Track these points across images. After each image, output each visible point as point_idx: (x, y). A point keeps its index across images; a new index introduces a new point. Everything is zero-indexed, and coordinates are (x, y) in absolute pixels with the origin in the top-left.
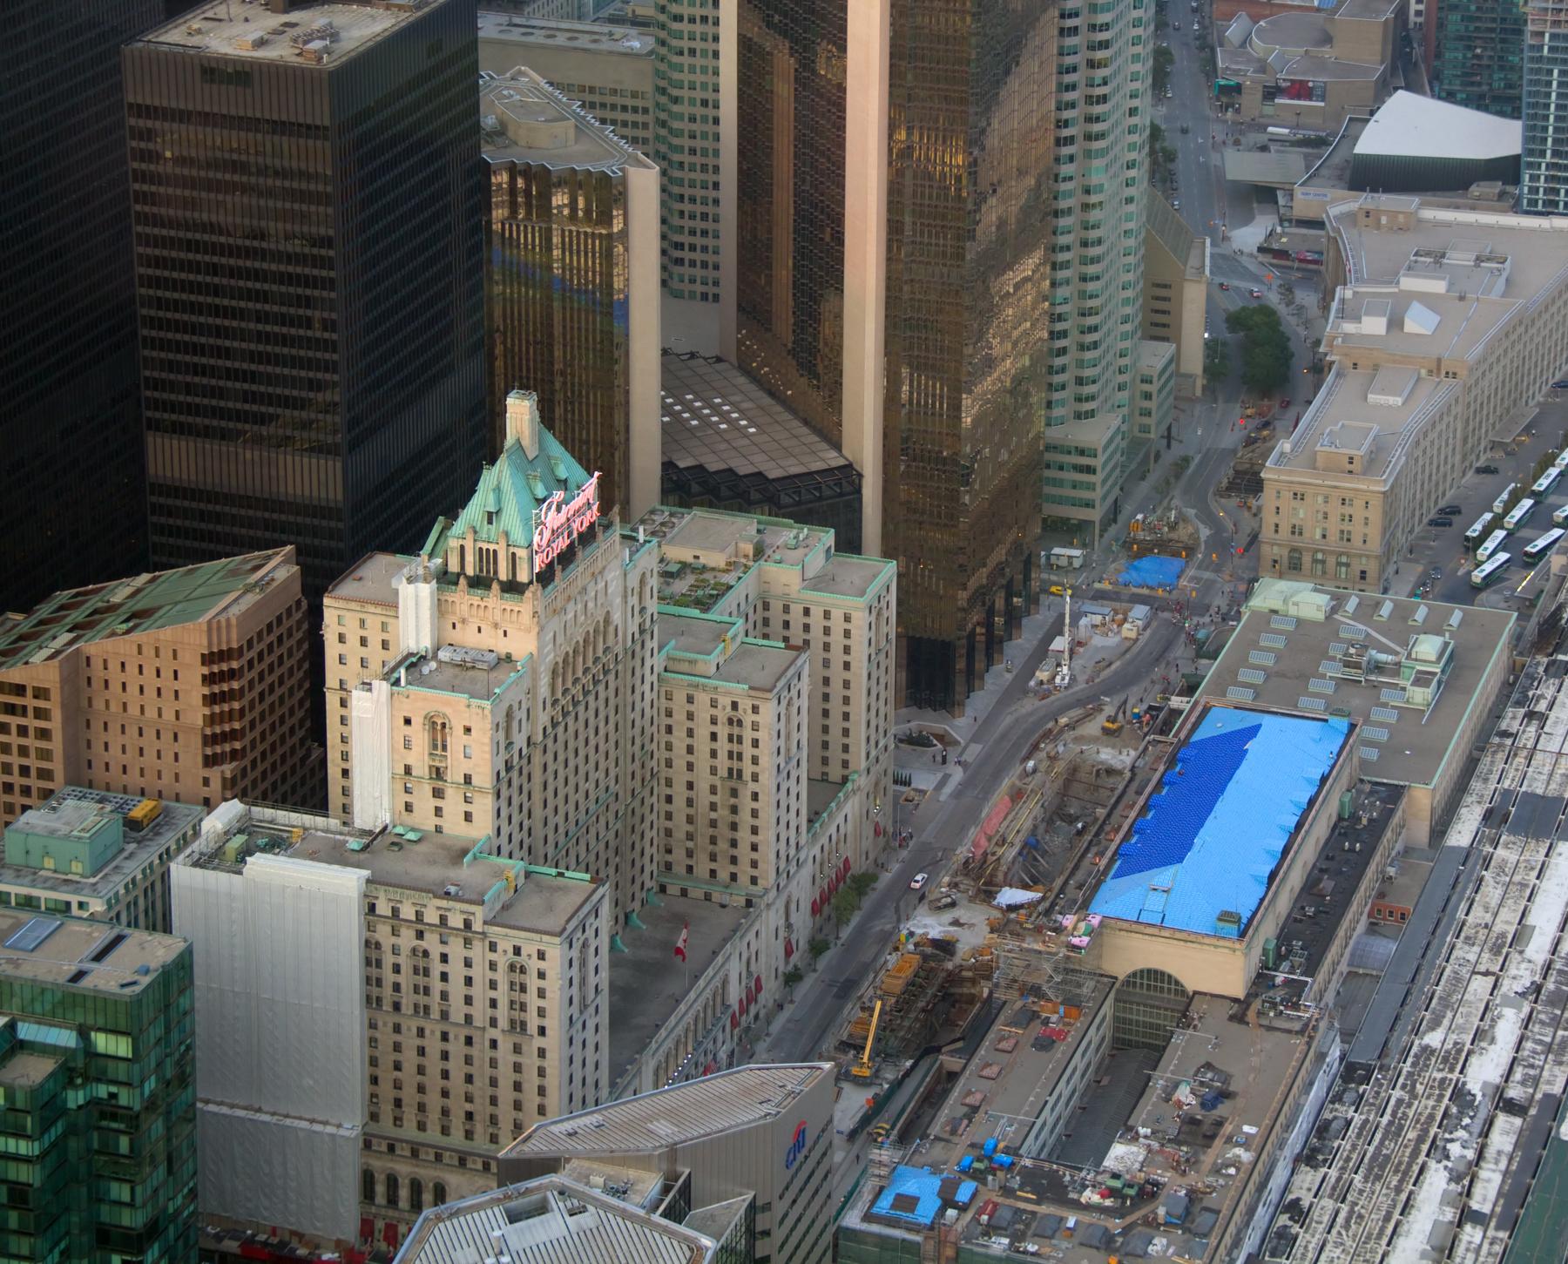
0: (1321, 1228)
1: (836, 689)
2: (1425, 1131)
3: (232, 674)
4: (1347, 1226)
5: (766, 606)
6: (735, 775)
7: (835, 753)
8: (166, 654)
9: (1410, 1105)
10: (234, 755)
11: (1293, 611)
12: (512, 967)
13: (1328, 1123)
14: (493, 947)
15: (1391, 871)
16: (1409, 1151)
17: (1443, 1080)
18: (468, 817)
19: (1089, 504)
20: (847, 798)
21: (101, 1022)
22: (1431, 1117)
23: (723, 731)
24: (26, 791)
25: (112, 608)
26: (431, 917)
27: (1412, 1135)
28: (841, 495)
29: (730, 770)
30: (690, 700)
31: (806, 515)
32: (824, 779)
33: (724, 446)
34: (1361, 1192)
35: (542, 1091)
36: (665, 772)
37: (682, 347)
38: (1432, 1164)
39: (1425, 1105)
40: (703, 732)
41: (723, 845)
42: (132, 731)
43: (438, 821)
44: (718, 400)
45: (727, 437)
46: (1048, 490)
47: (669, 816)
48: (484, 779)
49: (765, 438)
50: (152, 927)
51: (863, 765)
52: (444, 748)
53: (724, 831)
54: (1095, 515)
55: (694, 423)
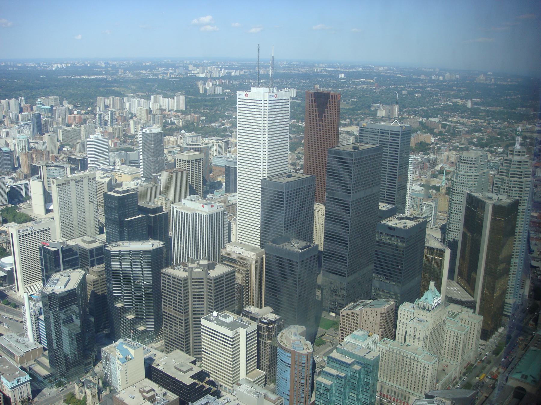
23: (455, 338)
24: (353, 328)
26: (412, 357)
31: (469, 307)
35: (426, 386)
48: (421, 338)
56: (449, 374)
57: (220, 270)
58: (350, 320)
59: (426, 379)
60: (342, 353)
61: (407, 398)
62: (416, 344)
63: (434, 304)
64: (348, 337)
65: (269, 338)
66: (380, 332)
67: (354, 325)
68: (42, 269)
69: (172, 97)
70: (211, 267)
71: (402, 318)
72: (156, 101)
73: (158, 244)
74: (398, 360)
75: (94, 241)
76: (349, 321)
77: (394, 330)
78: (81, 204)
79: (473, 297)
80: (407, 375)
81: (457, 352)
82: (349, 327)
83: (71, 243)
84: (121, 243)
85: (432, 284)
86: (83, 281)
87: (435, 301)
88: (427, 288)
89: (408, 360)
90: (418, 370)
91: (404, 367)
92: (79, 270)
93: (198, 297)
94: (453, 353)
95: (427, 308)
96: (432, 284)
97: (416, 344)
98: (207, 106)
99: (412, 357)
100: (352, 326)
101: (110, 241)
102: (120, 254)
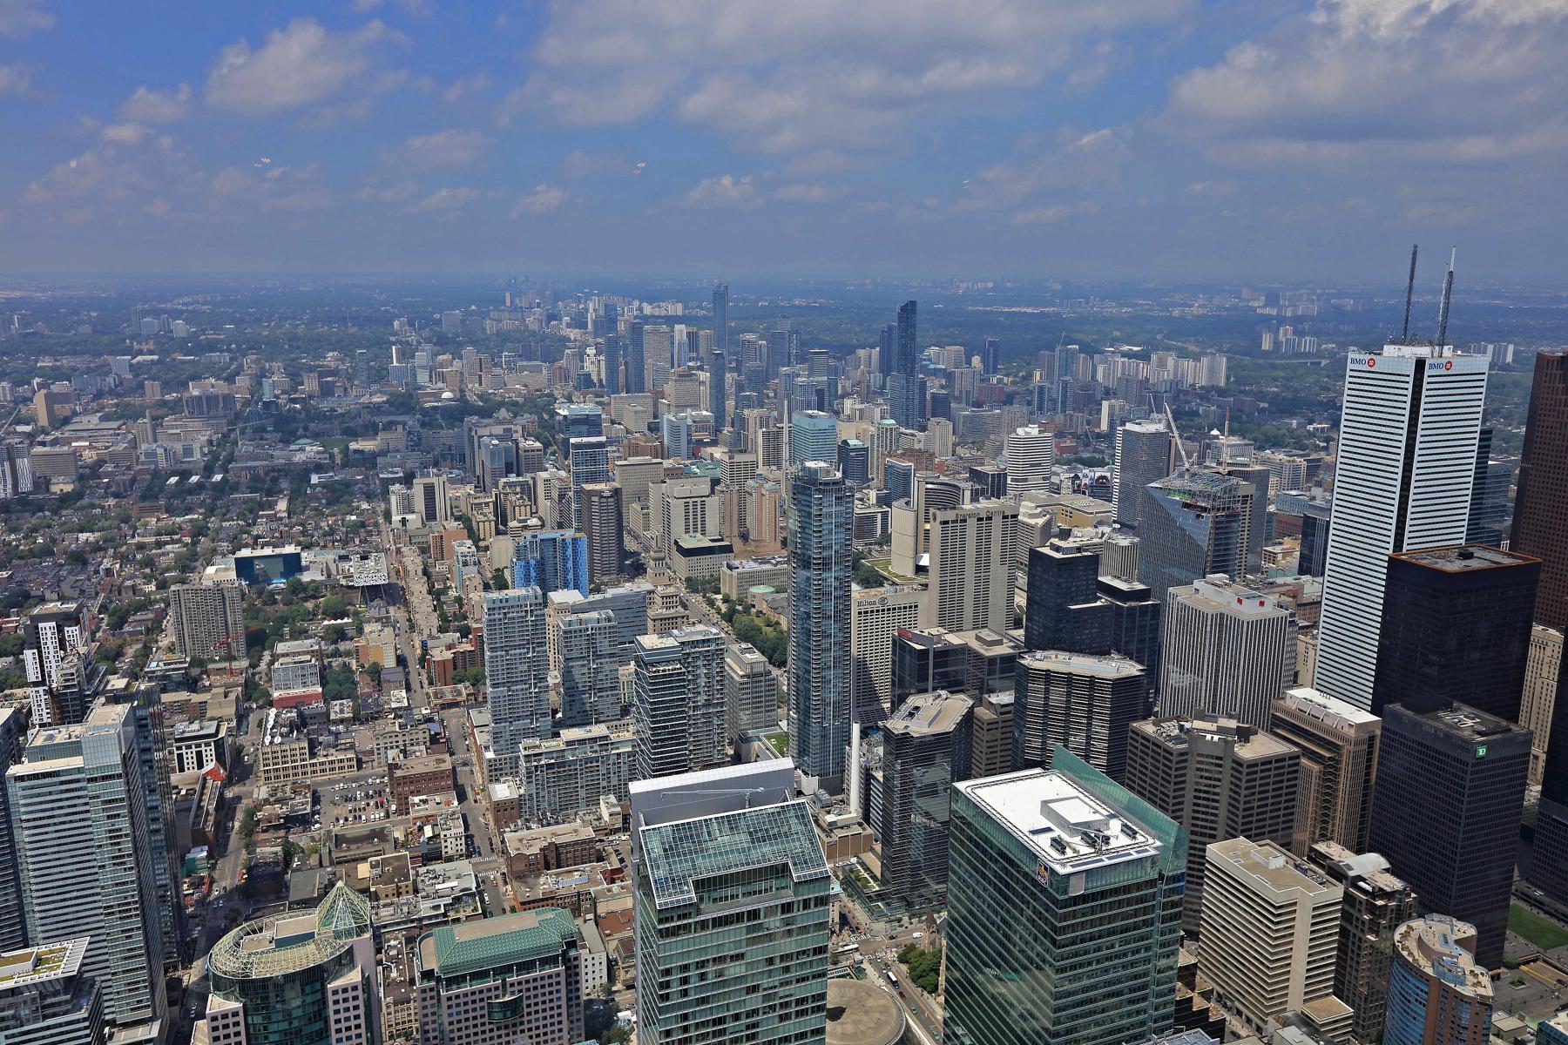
57: (1262, 747)
65: (1371, 931)
68: (893, 682)
69: (1197, 358)
70: (1244, 735)
72: (1162, 364)
73: (1132, 669)
75: (999, 643)
78: (983, 563)
83: (954, 639)
84: (1052, 653)
86: (969, 717)
92: (962, 696)
93: (1205, 797)
98: (1275, 379)
101: (1032, 645)
102: (1048, 676)
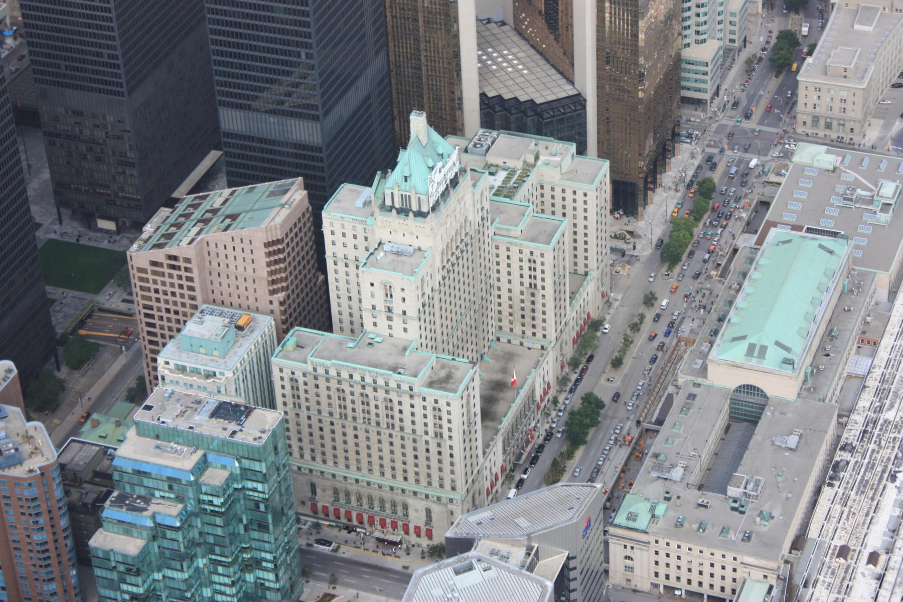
0: (835, 520)
1: (580, 230)
2: (886, 467)
3: (280, 251)
4: (848, 519)
5: (542, 187)
6: (533, 286)
7: (581, 261)
8: (246, 241)
9: (878, 452)
10: (283, 289)
11: (816, 164)
12: (434, 409)
13: (837, 463)
14: (424, 399)
15: (869, 319)
16: (878, 477)
17: (895, 438)
18: (405, 330)
19: (705, 91)
20: (588, 284)
21: (246, 456)
22: (889, 459)
23: (526, 265)
25: (214, 212)
27: (880, 469)
28: (575, 111)
29: (530, 284)
30: (508, 250)
32: (575, 272)
33: (511, 83)
34: (855, 500)
36: (496, 284)
37: (484, 16)
38: (889, 484)
39: (886, 453)
40: (515, 265)
41: (528, 319)
42: (232, 277)
43: (390, 331)
44: (505, 52)
45: (512, 76)
46: (683, 83)
47: (500, 304)
48: (412, 312)
49: (532, 77)
50: (264, 405)
51: (596, 265)
52: (391, 296)
53: (528, 313)
54: (707, 96)
55: (494, 67)
56: (523, 393)
58: (167, 279)
59: (449, 443)
60: (157, 437)
61: (399, 508)
62: (398, 331)
63: (435, 191)
64: (171, 346)
66: (276, 306)
67: (182, 296)
71: (339, 244)
74: (349, 398)
76: (164, 284)
77: (321, 277)
79: (572, 83)
80: (385, 438)
81: (539, 307)
82: (167, 302)
85: (418, 122)
87: (438, 177)
88: (401, 140)
89: (381, 394)
90: (419, 419)
91: (373, 417)
94: (528, 313)
95: (415, 208)
96: (418, 122)
97: (398, 331)
99: (393, 385)
100: (178, 299)
